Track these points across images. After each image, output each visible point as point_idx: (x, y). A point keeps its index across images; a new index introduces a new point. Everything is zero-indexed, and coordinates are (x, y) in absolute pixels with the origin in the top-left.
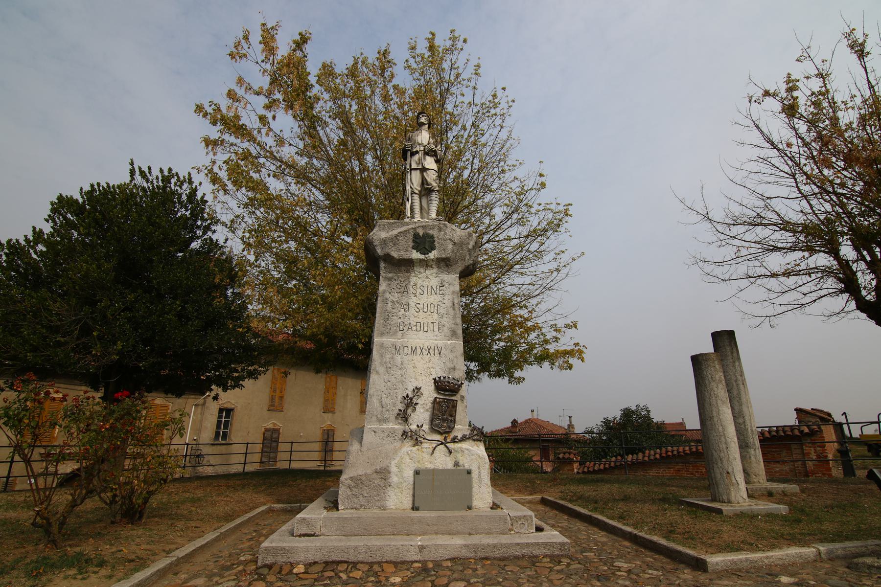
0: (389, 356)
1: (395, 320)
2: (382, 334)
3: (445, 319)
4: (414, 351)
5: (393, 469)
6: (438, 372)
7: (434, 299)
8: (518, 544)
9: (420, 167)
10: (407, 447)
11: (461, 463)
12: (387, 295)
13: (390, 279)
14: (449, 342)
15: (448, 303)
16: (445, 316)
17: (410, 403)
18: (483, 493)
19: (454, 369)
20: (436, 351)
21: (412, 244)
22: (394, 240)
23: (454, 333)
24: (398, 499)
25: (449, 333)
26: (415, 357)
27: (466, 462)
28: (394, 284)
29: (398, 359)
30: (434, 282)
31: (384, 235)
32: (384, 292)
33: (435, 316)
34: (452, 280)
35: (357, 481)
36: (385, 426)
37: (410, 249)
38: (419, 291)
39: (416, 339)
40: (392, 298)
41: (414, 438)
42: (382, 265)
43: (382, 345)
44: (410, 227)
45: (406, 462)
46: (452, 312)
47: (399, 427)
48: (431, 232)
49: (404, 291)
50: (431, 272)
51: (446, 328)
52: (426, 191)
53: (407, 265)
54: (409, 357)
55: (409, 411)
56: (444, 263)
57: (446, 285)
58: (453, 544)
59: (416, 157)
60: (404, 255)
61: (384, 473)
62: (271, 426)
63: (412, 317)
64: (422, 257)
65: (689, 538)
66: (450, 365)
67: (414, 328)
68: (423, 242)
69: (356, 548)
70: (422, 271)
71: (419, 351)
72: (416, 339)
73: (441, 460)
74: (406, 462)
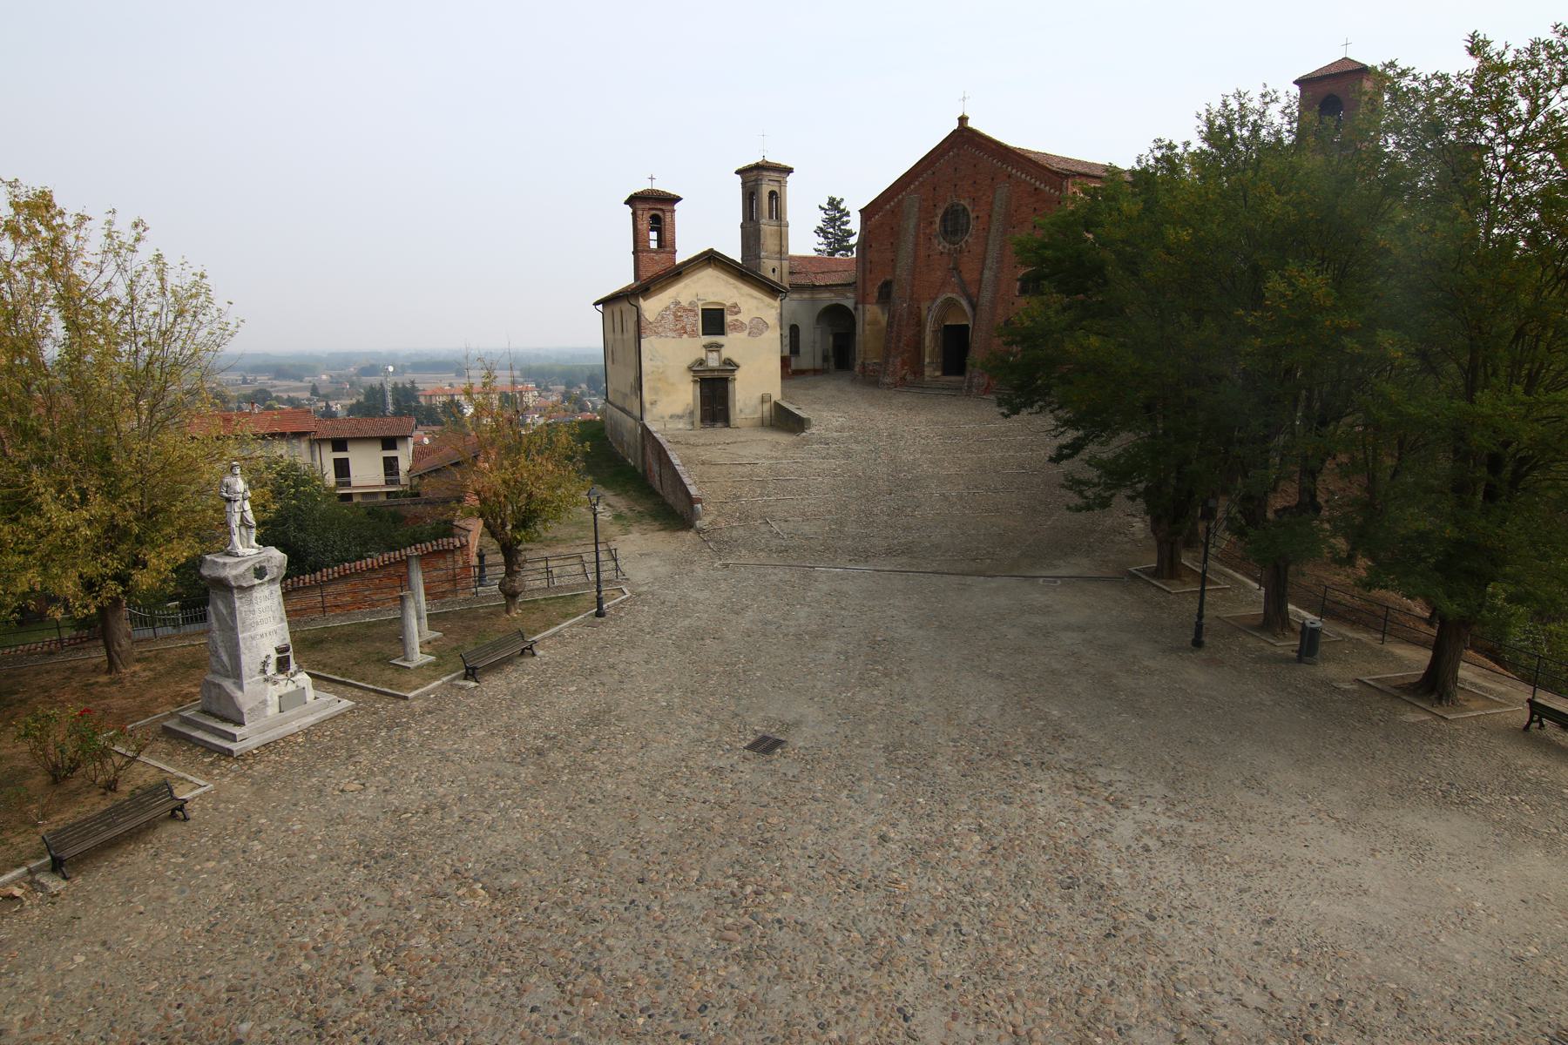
6: (277, 644)
7: (268, 603)
10: (270, 687)
17: (265, 663)
18: (310, 694)
22: (243, 576)
24: (272, 710)
27: (302, 685)
30: (267, 593)
31: (234, 572)
35: (252, 710)
44: (249, 564)
45: (273, 693)
47: (261, 677)
49: (251, 602)
52: (244, 523)
58: (310, 720)
61: (264, 702)
65: (400, 687)
72: (262, 629)
73: (291, 687)
74: (273, 693)
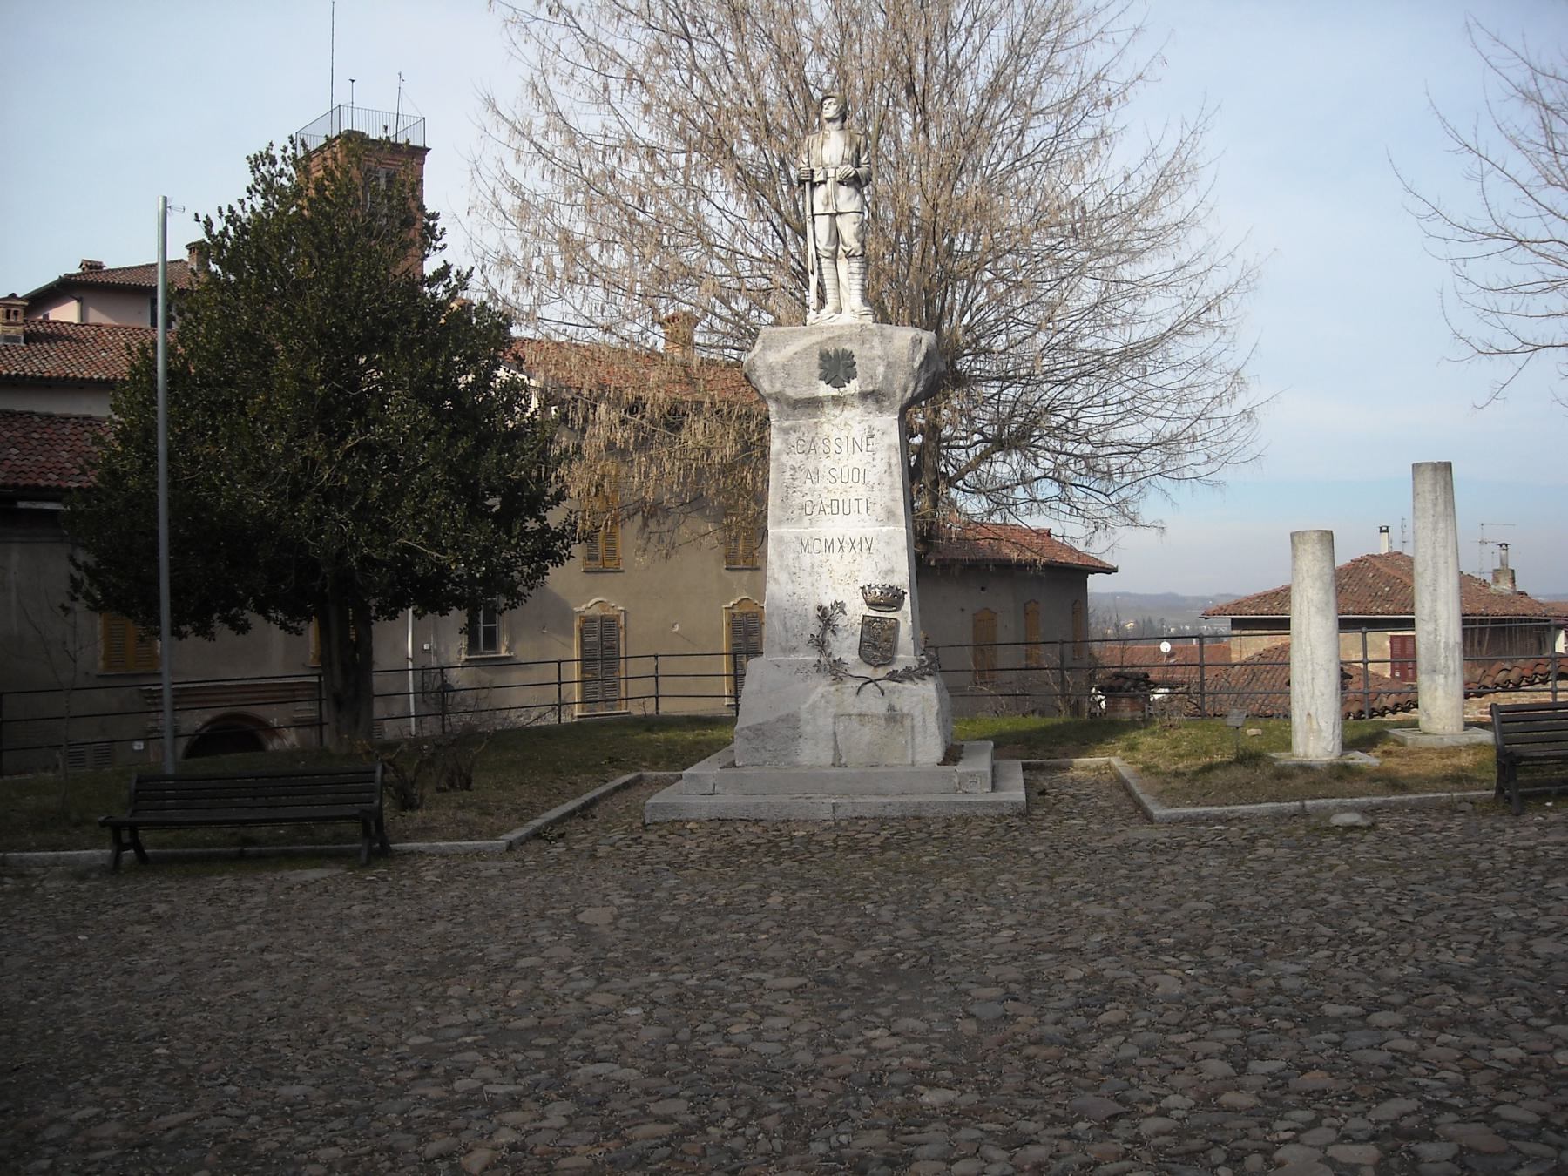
0: (792, 555)
1: (797, 499)
2: (780, 522)
3: (876, 492)
4: (829, 546)
5: (804, 716)
7: (857, 460)
8: (957, 803)
9: (831, 210)
10: (822, 687)
11: (897, 707)
12: (784, 458)
13: (786, 431)
14: (884, 529)
15: (882, 466)
16: (877, 487)
19: (892, 571)
20: (864, 546)
21: (818, 372)
23: (890, 514)
25: (883, 516)
26: (831, 556)
28: (793, 437)
29: (806, 559)
30: (857, 431)
32: (779, 454)
33: (861, 488)
34: (888, 424)
35: (758, 731)
36: (792, 658)
37: (815, 380)
38: (834, 447)
39: (832, 527)
40: (792, 462)
41: (836, 671)
42: (773, 408)
43: (781, 539)
44: (816, 338)
46: (887, 480)
47: (813, 657)
48: (848, 347)
49: (811, 449)
50: (849, 413)
51: (877, 507)
53: (813, 404)
54: (823, 556)
55: (829, 636)
56: (874, 397)
57: (878, 435)
59: (820, 193)
60: (803, 392)
62: (597, 611)
63: (824, 490)
64: (835, 392)
66: (885, 566)
67: (828, 510)
68: (837, 366)
69: (757, 806)
70: (837, 412)
71: (837, 545)
72: (832, 527)
